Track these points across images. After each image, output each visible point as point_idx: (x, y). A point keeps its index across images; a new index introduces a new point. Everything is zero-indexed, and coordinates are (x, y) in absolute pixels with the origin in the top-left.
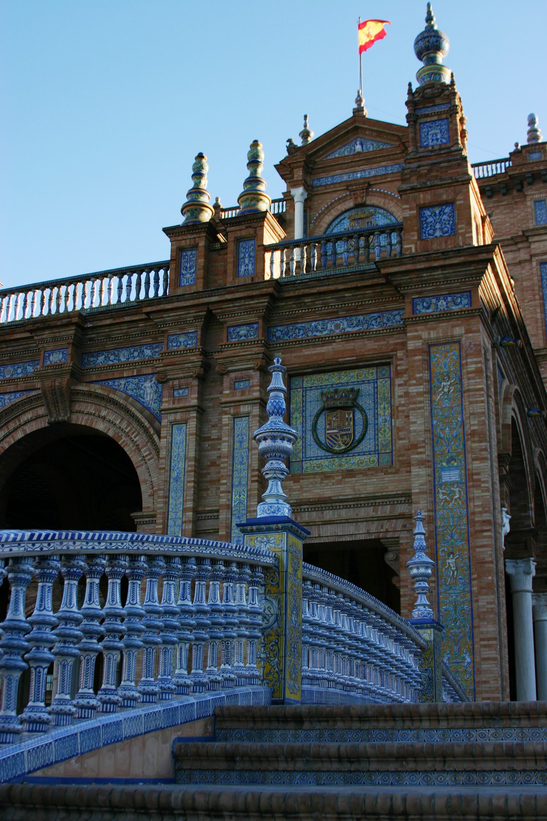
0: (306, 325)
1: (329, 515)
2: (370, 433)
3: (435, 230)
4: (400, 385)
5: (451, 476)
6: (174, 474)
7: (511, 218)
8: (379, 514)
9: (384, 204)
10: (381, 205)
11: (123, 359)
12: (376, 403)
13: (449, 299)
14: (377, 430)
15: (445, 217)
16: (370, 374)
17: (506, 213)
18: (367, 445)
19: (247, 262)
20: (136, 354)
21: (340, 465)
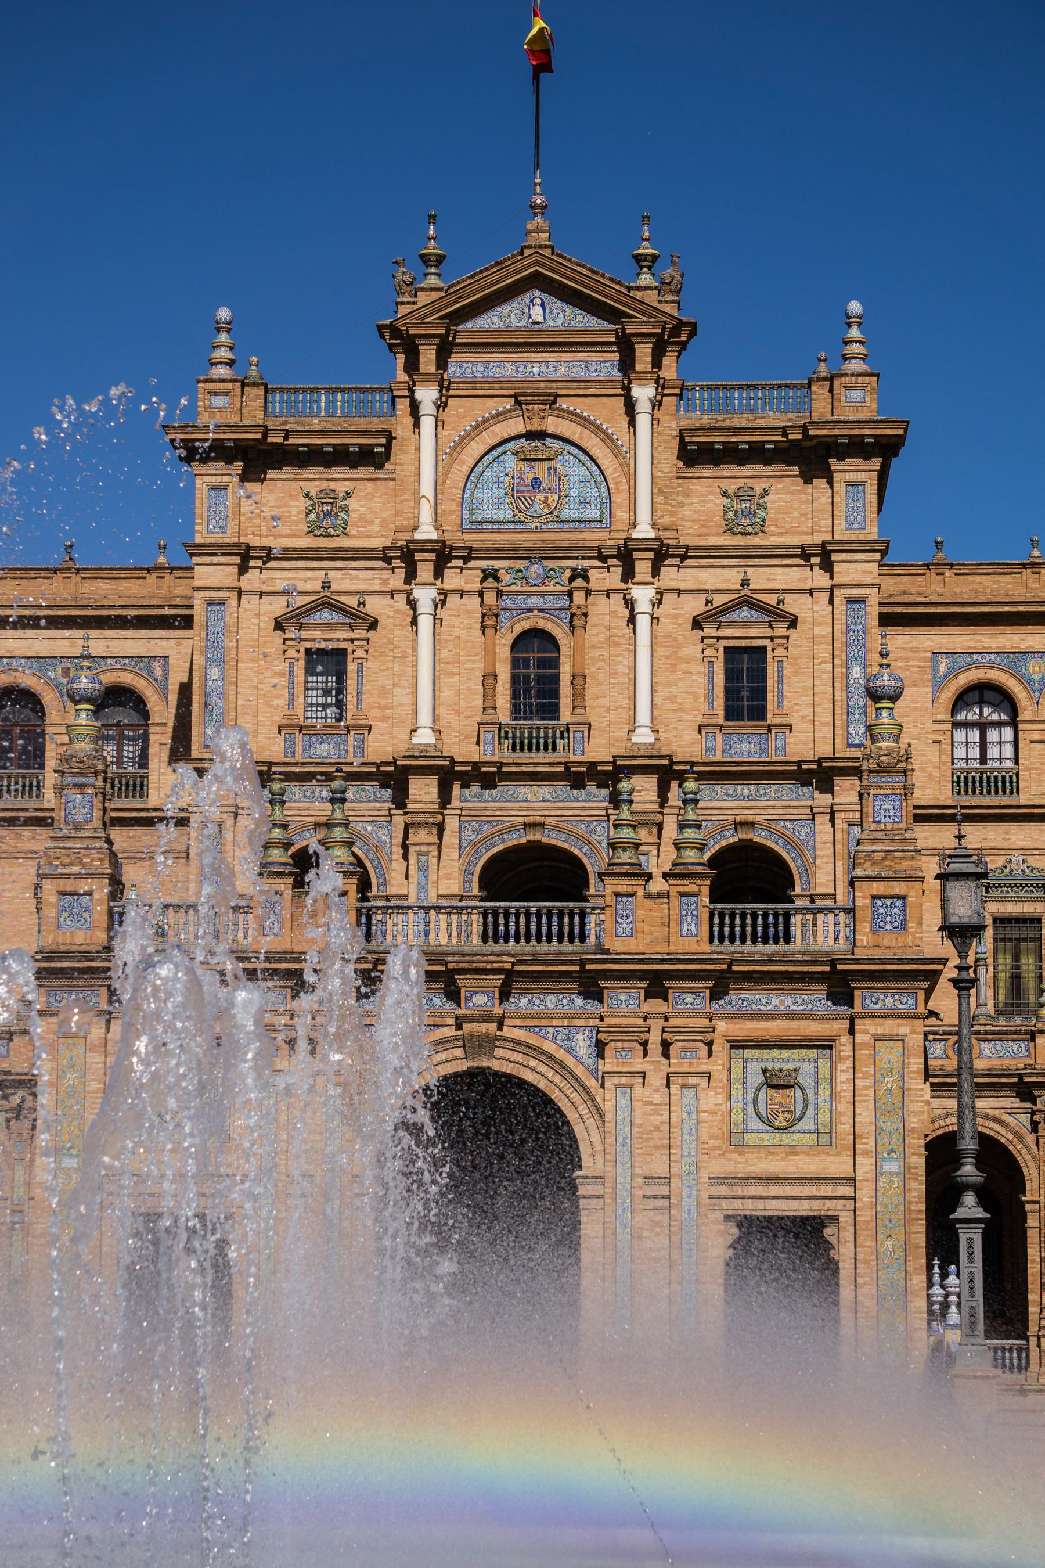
0: (751, 997)
1: (774, 1191)
2: (810, 1111)
3: (885, 923)
4: (842, 1071)
5: (892, 1167)
6: (620, 1139)
7: (802, 502)
8: (822, 1194)
9: (581, 438)
10: (575, 438)
11: (550, 1006)
12: (816, 1083)
13: (896, 997)
14: (816, 1109)
15: (896, 911)
16: (812, 1054)
17: (793, 493)
18: (806, 1123)
19: (689, 920)
20: (565, 1002)
21: (781, 1140)
